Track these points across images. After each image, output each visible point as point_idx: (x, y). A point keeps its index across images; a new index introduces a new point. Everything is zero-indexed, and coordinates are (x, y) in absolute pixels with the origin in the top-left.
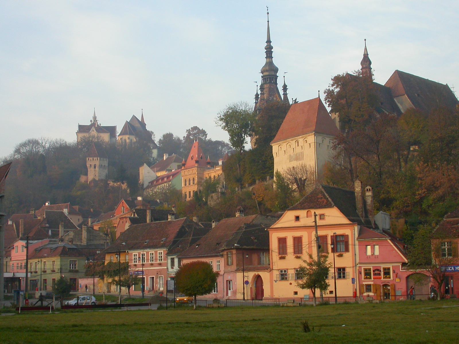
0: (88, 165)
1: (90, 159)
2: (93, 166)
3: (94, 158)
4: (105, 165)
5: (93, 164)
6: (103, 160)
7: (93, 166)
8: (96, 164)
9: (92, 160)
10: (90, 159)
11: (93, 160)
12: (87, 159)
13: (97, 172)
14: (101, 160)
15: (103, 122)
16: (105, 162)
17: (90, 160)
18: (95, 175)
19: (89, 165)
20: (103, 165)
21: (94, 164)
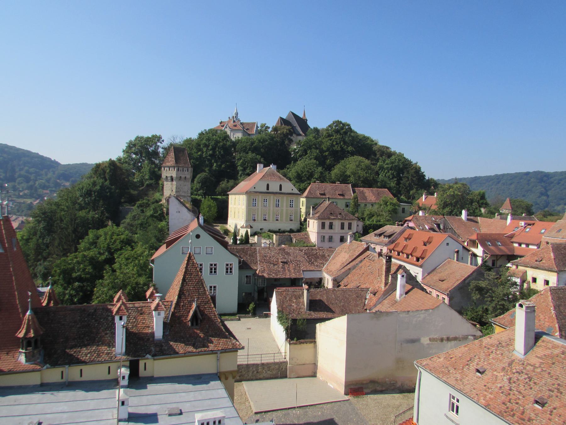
1: (166, 169)
2: (169, 178)
4: (185, 177)
5: (169, 175)
6: (183, 171)
7: (170, 178)
11: (169, 170)
12: (163, 169)
13: (175, 187)
15: (244, 119)
20: (183, 176)
21: (170, 176)
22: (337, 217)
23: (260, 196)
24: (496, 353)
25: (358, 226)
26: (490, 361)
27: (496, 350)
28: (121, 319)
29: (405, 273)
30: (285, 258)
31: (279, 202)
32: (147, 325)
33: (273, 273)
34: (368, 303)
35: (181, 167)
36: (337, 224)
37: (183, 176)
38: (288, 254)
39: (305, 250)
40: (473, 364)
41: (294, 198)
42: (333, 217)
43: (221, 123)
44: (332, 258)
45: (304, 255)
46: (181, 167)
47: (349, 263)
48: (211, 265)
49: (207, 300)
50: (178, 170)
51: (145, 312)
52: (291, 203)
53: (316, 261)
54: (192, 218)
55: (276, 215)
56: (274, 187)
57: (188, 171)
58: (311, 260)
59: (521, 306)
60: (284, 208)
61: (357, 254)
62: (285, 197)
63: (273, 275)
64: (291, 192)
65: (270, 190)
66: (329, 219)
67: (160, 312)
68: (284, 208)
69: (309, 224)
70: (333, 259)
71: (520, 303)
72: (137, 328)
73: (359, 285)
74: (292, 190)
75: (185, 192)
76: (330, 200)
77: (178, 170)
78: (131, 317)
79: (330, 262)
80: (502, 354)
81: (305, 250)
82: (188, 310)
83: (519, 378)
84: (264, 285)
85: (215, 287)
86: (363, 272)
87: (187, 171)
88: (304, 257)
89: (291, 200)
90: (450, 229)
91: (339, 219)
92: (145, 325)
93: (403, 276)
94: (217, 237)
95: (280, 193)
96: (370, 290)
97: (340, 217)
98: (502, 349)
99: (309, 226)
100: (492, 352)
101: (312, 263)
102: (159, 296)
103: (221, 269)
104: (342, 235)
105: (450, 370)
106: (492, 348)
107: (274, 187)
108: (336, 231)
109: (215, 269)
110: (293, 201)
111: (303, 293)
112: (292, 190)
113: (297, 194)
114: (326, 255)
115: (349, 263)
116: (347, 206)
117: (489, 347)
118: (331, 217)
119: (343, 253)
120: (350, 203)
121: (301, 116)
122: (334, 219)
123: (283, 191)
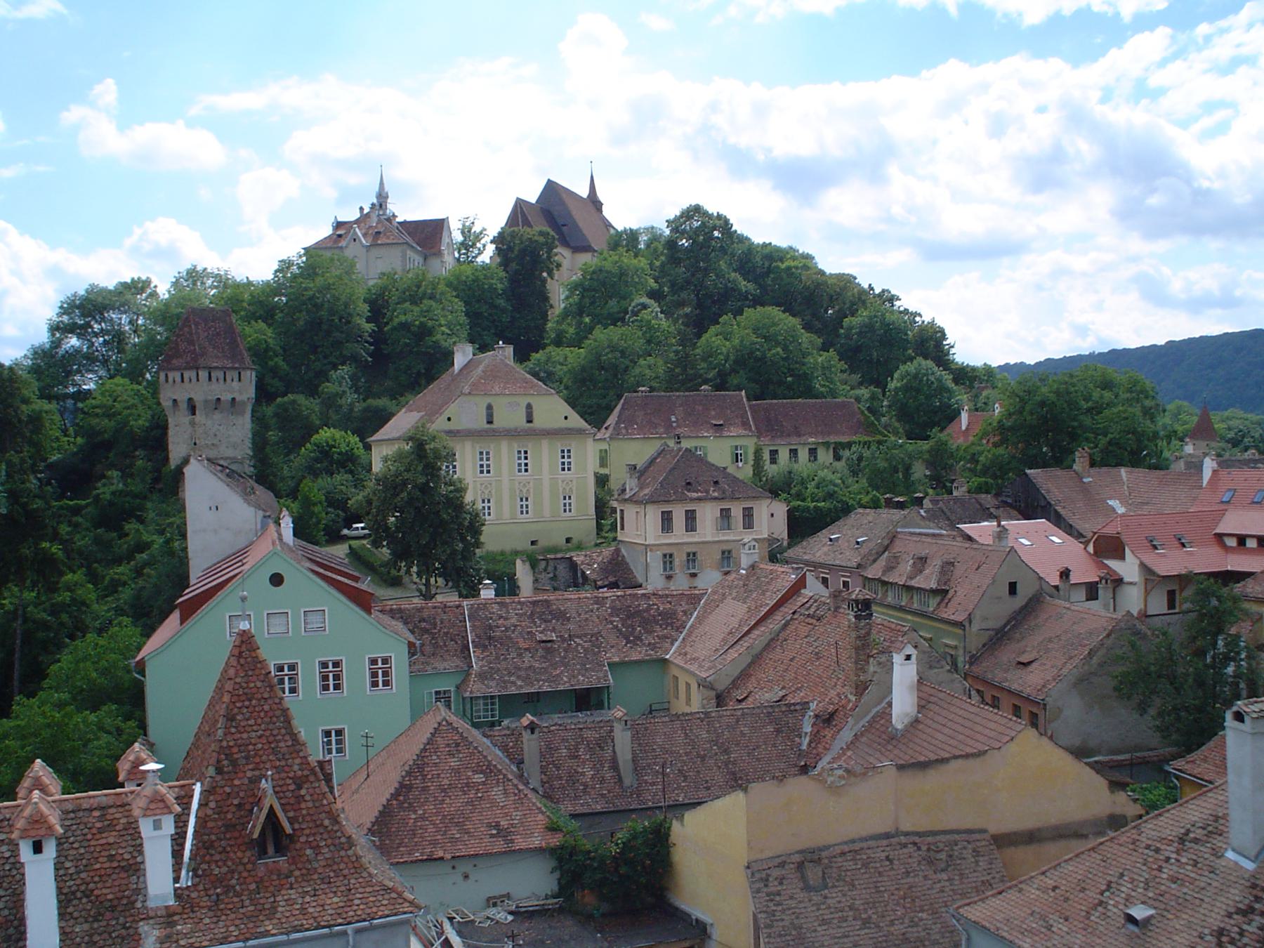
0: (166, 404)
1: (171, 375)
2: (183, 406)
3: (186, 375)
5: (182, 395)
6: (225, 380)
7: (185, 405)
8: (192, 396)
9: (178, 379)
10: (171, 375)
11: (183, 381)
14: (214, 379)
15: (405, 210)
16: (235, 383)
17: (170, 379)
18: (195, 444)
19: (170, 403)
20: (226, 397)
21: (186, 399)
22: (707, 492)
23: (468, 445)
24: (1178, 861)
25: (772, 515)
26: (1163, 888)
27: (1178, 852)
28: (38, 848)
29: (916, 647)
30: (554, 630)
31: (526, 458)
32: (123, 864)
33: (519, 677)
34: (809, 745)
35: (216, 368)
36: (708, 514)
37: (226, 397)
38: (562, 616)
39: (613, 601)
40: (1117, 899)
41: (574, 445)
42: (695, 495)
43: (339, 225)
44: (697, 617)
45: (611, 615)
46: (216, 368)
47: (749, 632)
48: (324, 665)
49: (306, 772)
50: (210, 379)
51: (115, 822)
52: (566, 460)
53: (650, 632)
54: (259, 526)
55: (522, 500)
56: (509, 415)
57: (240, 380)
58: (634, 629)
59: (1239, 717)
60: (546, 477)
61: (772, 603)
62: (545, 443)
63: (519, 683)
64: (564, 424)
65: (499, 423)
66: (683, 499)
67: (160, 820)
68: (546, 477)
69: (622, 518)
70: (700, 620)
71: (1235, 709)
72: (92, 874)
73: (781, 693)
74: (566, 418)
75: (235, 446)
76: (682, 440)
77: (210, 379)
78: (72, 839)
79: (690, 634)
80: (1195, 863)
81: (613, 601)
82: (248, 807)
83: (1245, 927)
84: (493, 716)
85: (339, 733)
86: (791, 655)
87: (236, 379)
88: (611, 622)
89: (563, 451)
90: (1042, 507)
91: (716, 498)
92: (115, 864)
93: (908, 658)
94: (339, 578)
95: (529, 432)
96: (813, 706)
97: (716, 494)
98: (1196, 847)
99: (622, 528)
100: (1168, 859)
101: (639, 638)
102: (154, 771)
103: (356, 675)
104: (725, 547)
105: (1051, 926)
106: (1168, 848)
107: (509, 415)
108: (709, 539)
109: (337, 677)
110: (569, 451)
111: (612, 731)
112: (566, 418)
113: (580, 432)
114: (680, 609)
115: (749, 632)
116: (736, 458)
117: (1158, 845)
118: (688, 494)
119: (729, 600)
120: (746, 447)
121: (584, 192)
122: (699, 499)
123: (539, 422)
